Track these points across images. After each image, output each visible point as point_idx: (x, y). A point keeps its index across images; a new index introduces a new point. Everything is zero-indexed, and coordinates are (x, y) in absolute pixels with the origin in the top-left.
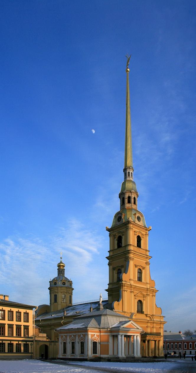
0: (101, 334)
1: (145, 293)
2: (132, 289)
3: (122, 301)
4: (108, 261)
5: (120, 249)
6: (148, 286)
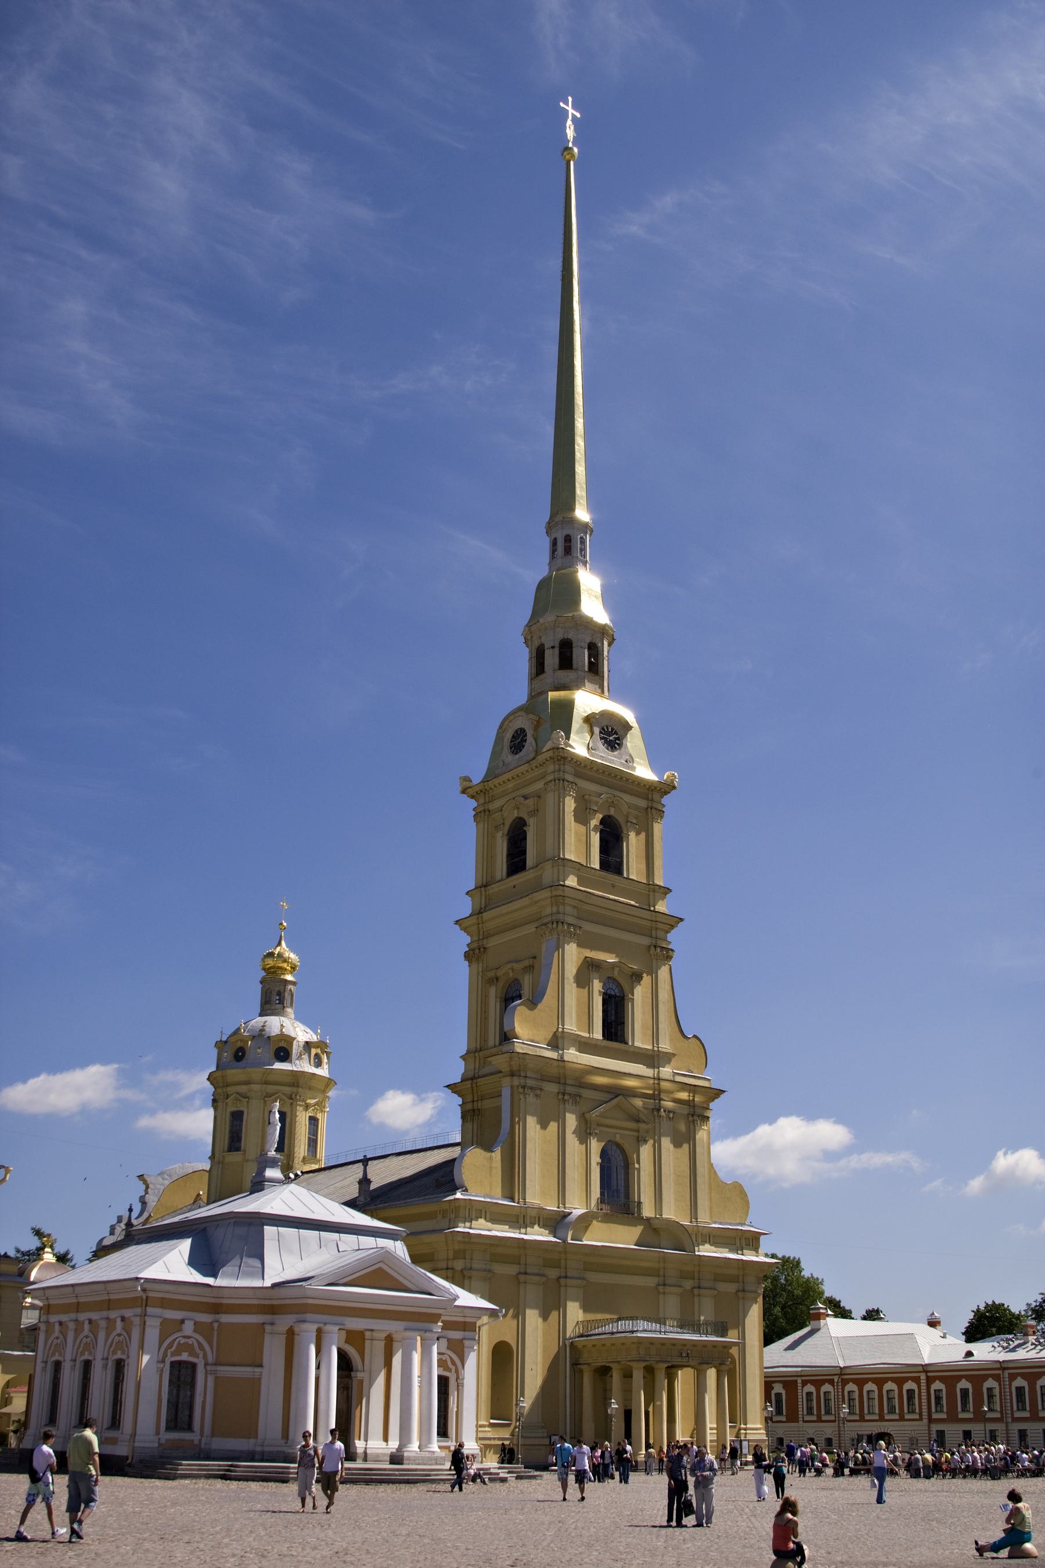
0: (226, 1318)
4: (468, 940)
5: (519, 878)
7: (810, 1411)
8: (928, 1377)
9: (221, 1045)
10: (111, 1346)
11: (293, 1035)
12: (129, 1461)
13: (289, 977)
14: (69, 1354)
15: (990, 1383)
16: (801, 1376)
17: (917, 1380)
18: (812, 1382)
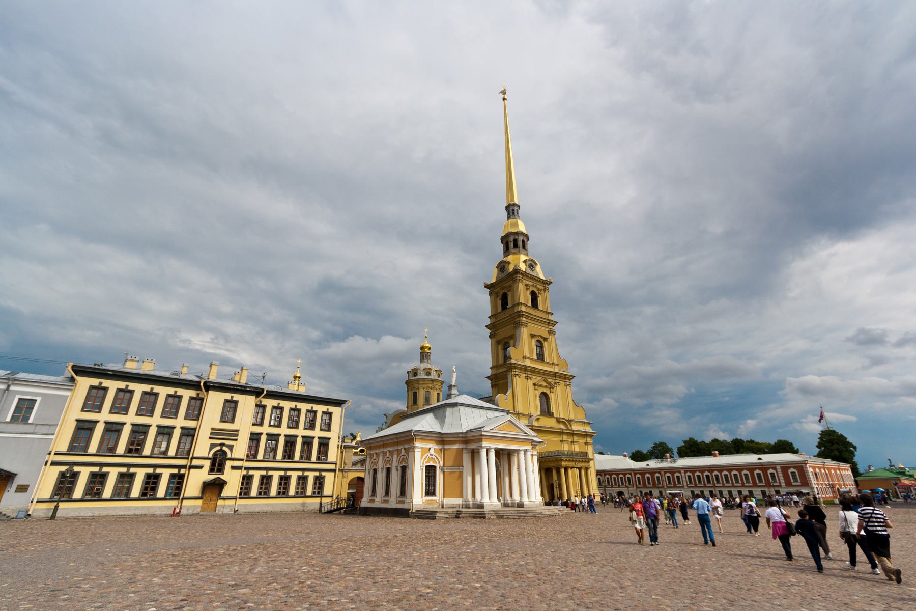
0: (446, 447)
1: (553, 381)
2: (529, 373)
3: (511, 394)
5: (506, 311)
6: (556, 369)
10: (399, 460)
12: (410, 511)
14: (380, 465)
15: (657, 475)
17: (630, 474)
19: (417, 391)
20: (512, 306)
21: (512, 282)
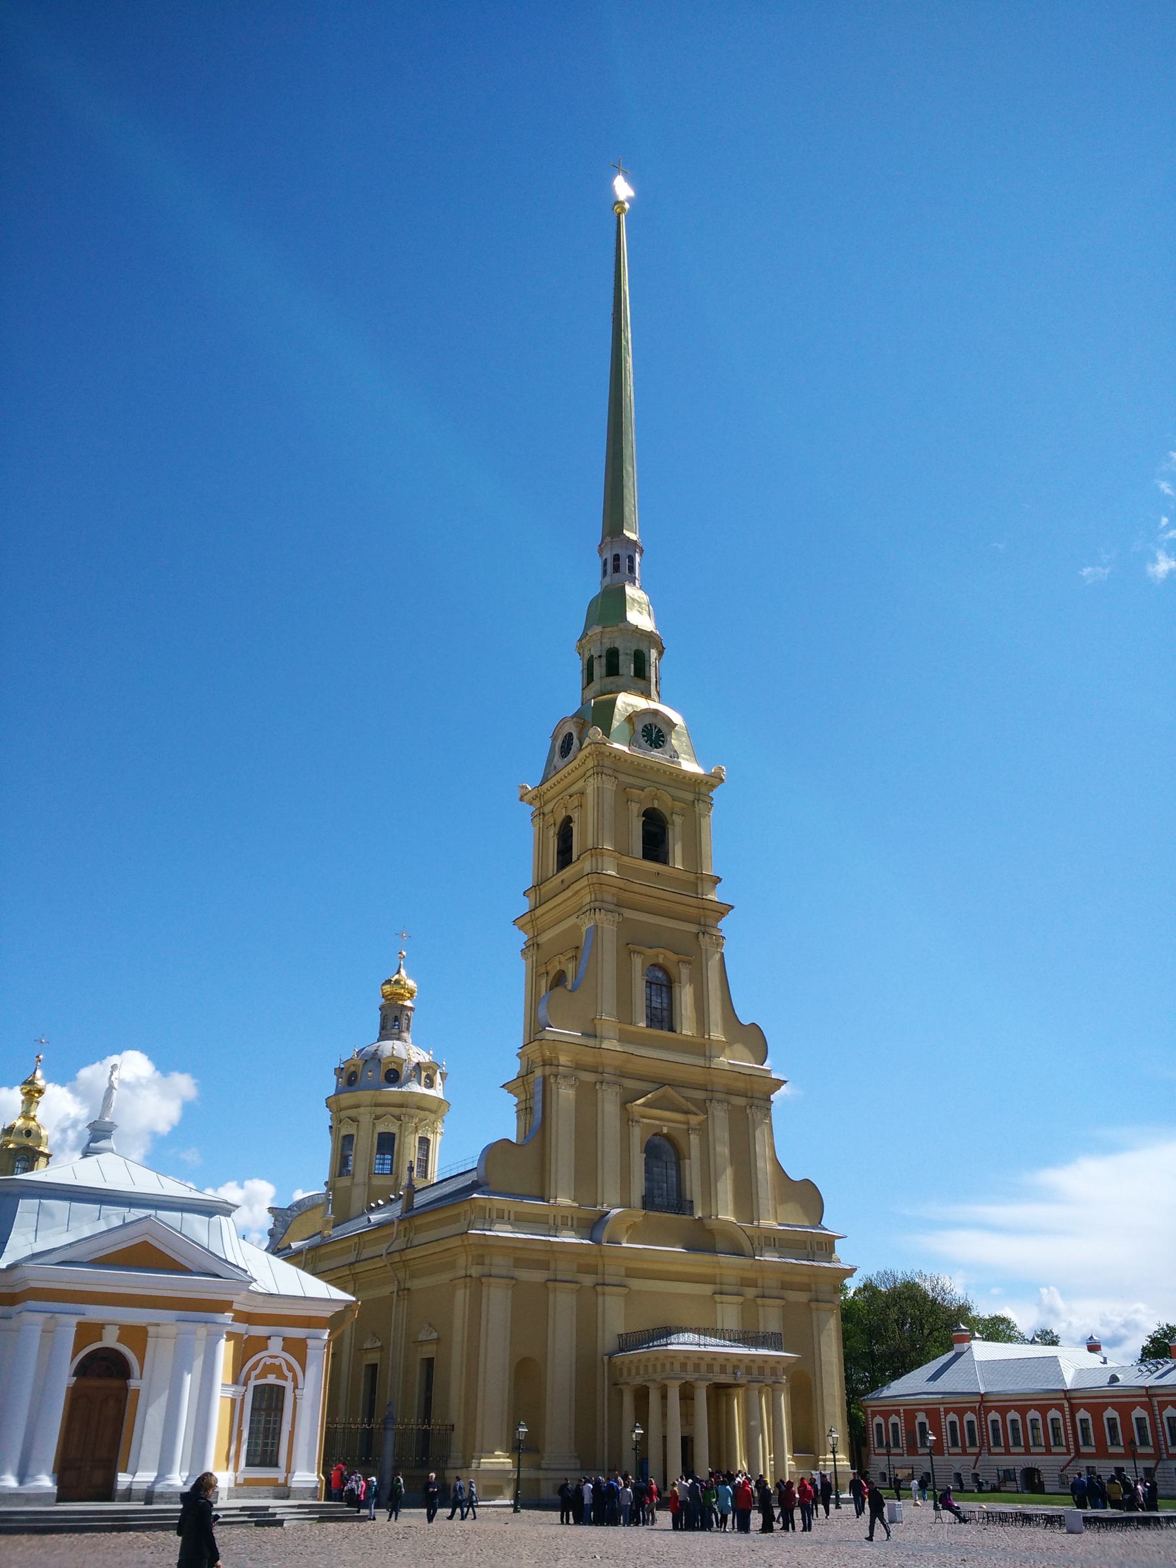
4: (526, 938)
7: (955, 1444)
8: (1071, 1406)
9: (339, 1071)
11: (404, 1056)
13: (408, 1003)
16: (943, 1403)
17: (1060, 1408)
18: (955, 1410)
19: (352, 1131)
20: (578, 859)
21: (581, 783)
